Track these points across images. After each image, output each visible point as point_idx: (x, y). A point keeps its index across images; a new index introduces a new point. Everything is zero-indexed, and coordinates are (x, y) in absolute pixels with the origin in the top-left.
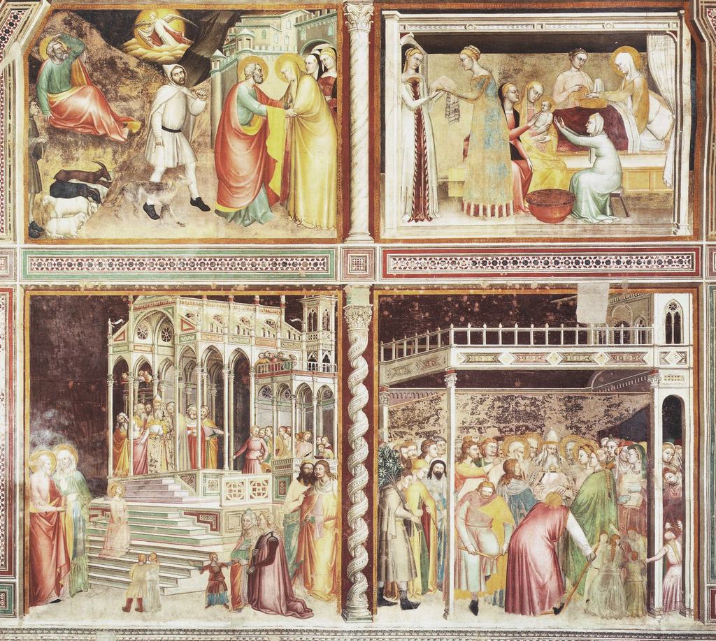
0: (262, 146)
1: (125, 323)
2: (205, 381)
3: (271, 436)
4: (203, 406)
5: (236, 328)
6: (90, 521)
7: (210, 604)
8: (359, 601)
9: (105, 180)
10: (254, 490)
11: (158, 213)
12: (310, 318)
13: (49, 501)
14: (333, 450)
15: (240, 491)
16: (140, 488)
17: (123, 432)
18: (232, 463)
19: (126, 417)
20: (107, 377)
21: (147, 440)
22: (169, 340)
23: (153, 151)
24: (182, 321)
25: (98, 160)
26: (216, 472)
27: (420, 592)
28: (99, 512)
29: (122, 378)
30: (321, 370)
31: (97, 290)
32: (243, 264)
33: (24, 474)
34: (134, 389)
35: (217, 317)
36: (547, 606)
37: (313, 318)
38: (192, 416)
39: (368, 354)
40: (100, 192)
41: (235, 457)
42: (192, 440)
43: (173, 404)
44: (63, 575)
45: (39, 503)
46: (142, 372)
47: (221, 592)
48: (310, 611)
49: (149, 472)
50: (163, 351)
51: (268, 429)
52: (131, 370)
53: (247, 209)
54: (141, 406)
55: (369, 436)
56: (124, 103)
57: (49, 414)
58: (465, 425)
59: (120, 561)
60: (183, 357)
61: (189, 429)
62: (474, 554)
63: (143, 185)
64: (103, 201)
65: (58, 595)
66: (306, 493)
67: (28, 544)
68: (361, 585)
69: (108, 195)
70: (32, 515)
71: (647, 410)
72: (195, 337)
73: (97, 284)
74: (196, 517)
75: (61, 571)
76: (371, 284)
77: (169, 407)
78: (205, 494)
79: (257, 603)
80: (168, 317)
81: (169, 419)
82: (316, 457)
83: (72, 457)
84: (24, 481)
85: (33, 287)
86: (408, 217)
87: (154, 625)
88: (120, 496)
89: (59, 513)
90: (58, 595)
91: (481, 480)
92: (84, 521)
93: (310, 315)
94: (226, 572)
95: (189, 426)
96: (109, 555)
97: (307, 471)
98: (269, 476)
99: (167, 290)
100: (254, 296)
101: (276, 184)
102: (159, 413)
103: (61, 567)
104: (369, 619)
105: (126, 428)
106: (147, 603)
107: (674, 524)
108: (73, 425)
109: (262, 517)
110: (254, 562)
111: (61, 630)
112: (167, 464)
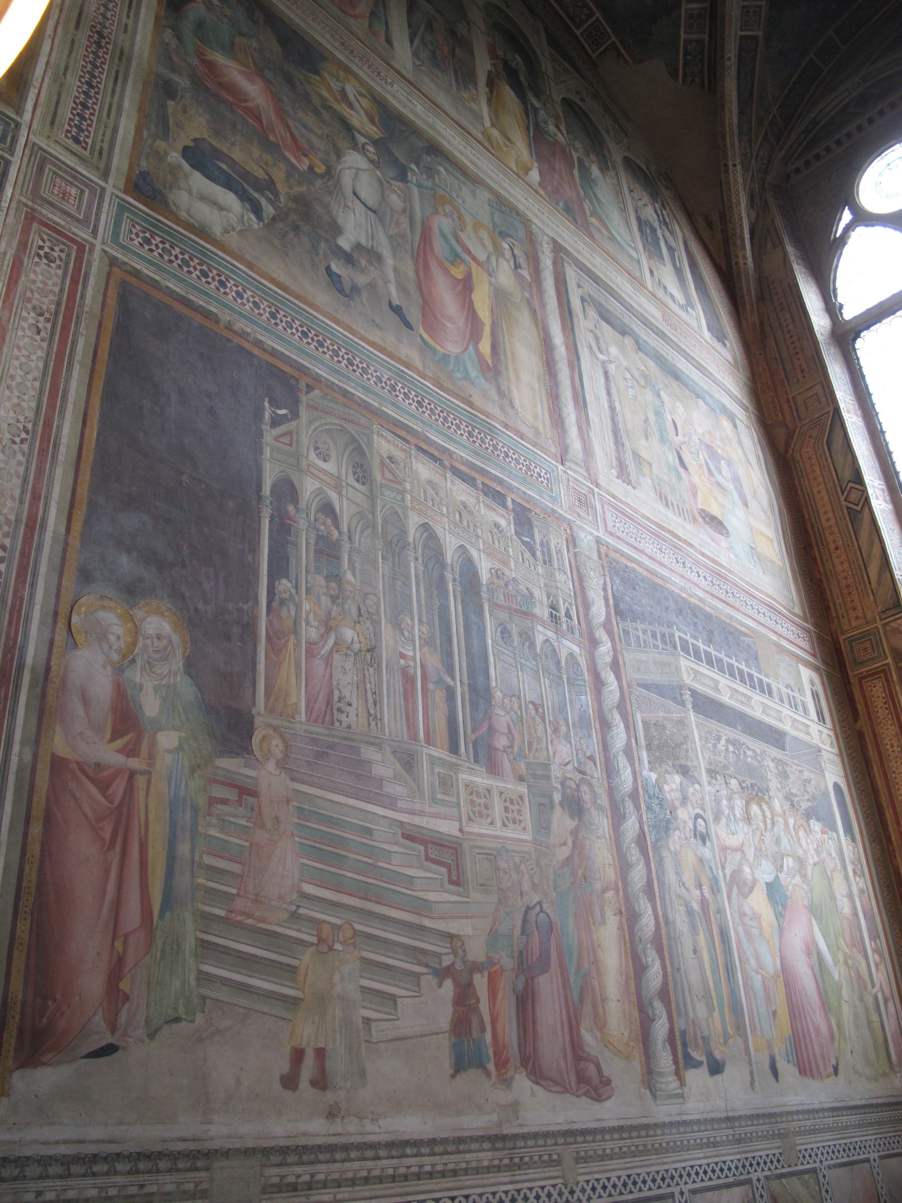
0: (467, 301)
1: (292, 419)
2: (421, 577)
3: (519, 713)
4: (420, 620)
5: (457, 515)
6: (210, 815)
7: (459, 1067)
8: (664, 1060)
9: (273, 198)
10: (506, 809)
11: (348, 292)
12: (542, 544)
13: (108, 735)
14: (595, 764)
15: (487, 807)
16: (320, 755)
17: (287, 613)
18: (471, 745)
19: (293, 591)
20: (260, 498)
21: (331, 653)
22: (363, 484)
23: (341, 209)
24: (382, 463)
25: (264, 166)
26: (449, 759)
27: (722, 1040)
28: (232, 795)
29: (287, 512)
30: (565, 627)
31: (248, 341)
32: (458, 427)
33: (52, 642)
34: (307, 543)
35: (430, 482)
36: (827, 1063)
37: (545, 545)
38: (406, 633)
39: (607, 626)
40: (264, 207)
41: (473, 737)
42: (408, 680)
43: (374, 598)
44: (130, 962)
45: (81, 733)
46: (321, 517)
47: (475, 1035)
48: (607, 1082)
49: (337, 724)
50: (356, 492)
51: (514, 699)
52: (303, 505)
53: (457, 358)
54: (320, 580)
55: (628, 752)
56: (304, 131)
57: (131, 521)
58: (713, 767)
59: (277, 935)
60: (385, 522)
61: (403, 656)
62: (758, 973)
63: (327, 241)
64: (266, 221)
65: (113, 1027)
66: (575, 833)
67: (35, 849)
68: (661, 1028)
69: (273, 218)
70: (58, 764)
71: (826, 794)
72: (403, 499)
73: (249, 330)
74: (422, 848)
75: (125, 949)
76: (596, 533)
77: (369, 602)
78: (434, 801)
79: (534, 1063)
80: (361, 447)
81: (368, 624)
82: (580, 772)
83: (176, 639)
84: (49, 660)
85: (129, 268)
86: (614, 472)
87: (351, 1128)
88: (278, 764)
89: (132, 774)
90: (113, 1027)
91: (738, 856)
92: (195, 809)
93: (542, 541)
94: (481, 983)
95: (402, 650)
96: (250, 916)
97: (569, 791)
98: (523, 789)
99: (359, 405)
100: (474, 479)
101: (485, 346)
102: (351, 607)
103: (126, 936)
104: (677, 1096)
105: (293, 613)
106: (337, 1064)
107: (875, 941)
108: (184, 566)
109: (523, 867)
110: (522, 963)
111: (105, 1159)
112: (370, 715)
